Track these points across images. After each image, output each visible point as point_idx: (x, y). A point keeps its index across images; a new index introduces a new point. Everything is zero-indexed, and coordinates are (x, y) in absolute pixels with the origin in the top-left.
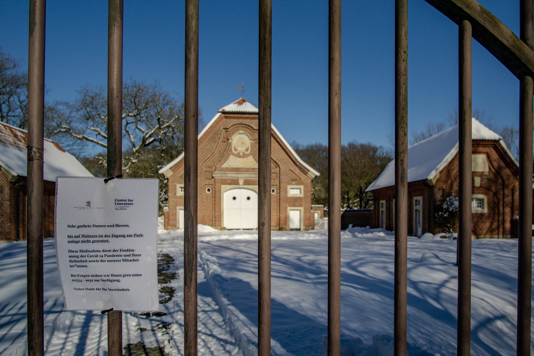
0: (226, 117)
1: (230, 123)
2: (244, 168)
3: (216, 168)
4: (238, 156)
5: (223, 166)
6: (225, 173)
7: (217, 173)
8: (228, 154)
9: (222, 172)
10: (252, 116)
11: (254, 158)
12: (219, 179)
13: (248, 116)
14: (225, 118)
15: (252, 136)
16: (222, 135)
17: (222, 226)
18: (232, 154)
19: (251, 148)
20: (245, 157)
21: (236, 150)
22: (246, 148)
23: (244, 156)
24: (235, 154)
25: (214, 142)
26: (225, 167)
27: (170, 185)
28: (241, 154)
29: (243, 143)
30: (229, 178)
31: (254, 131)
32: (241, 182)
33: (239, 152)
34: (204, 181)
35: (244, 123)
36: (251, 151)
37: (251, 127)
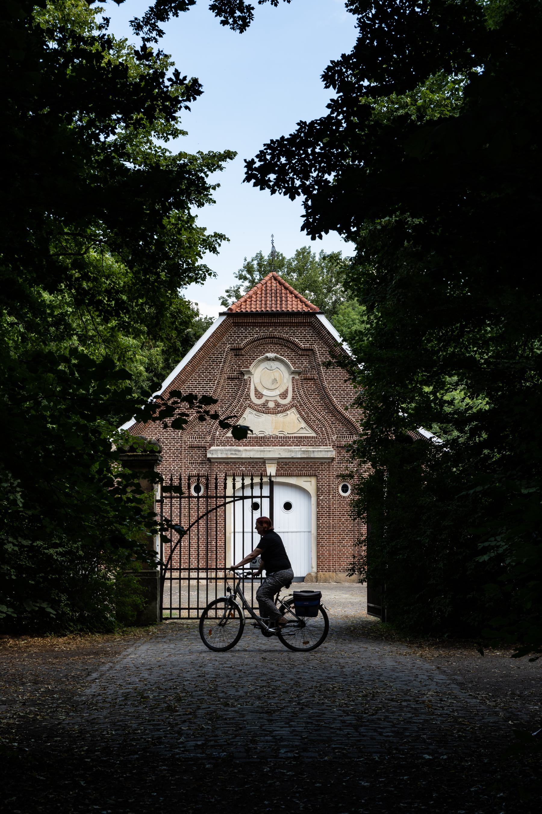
0: (237, 325)
1: (246, 337)
2: (277, 437)
3: (213, 439)
4: (264, 409)
6: (236, 450)
7: (216, 451)
8: (242, 405)
9: (228, 447)
10: (295, 320)
11: (300, 414)
13: (286, 320)
14: (235, 326)
15: (294, 364)
16: (227, 364)
18: (250, 406)
19: (294, 391)
20: (279, 412)
21: (259, 395)
22: (282, 390)
23: (279, 410)
24: (256, 405)
25: (210, 380)
28: (271, 405)
29: (275, 381)
30: (243, 461)
31: (300, 352)
32: (271, 470)
33: (267, 401)
34: (188, 468)
36: (293, 398)
37: (293, 343)
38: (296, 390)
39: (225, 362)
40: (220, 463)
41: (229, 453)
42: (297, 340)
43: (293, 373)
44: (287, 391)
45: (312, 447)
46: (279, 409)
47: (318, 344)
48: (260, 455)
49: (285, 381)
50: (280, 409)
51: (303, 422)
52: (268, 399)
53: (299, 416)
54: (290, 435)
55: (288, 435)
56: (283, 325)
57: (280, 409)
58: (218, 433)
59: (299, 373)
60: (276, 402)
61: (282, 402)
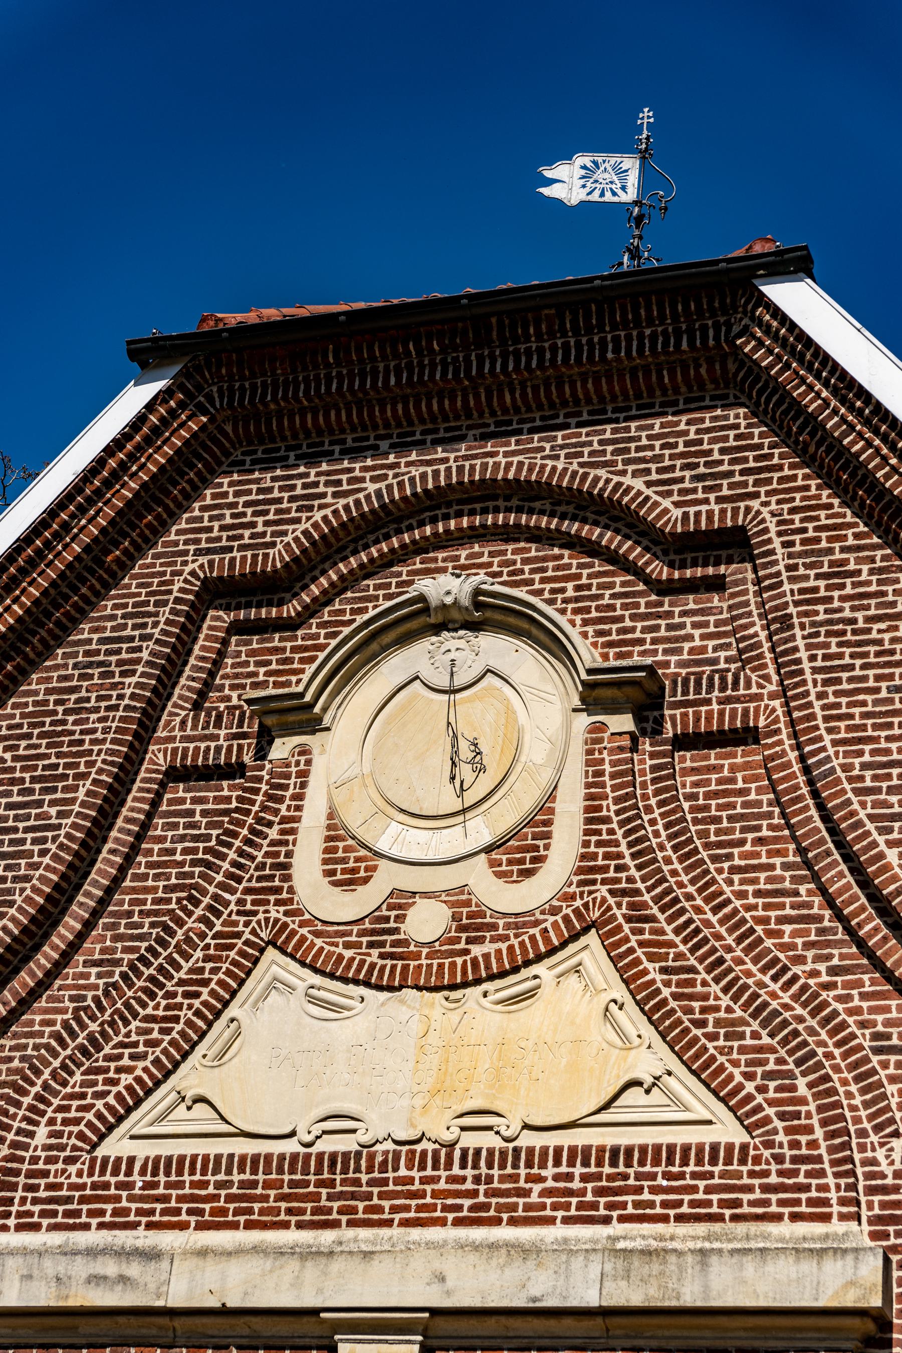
9: (94, 1237)
25: (49, 781)
26: (144, 1150)
38: (609, 808)
41: (81, 1268)
42: (638, 484)
45: (701, 1228)
46: (477, 950)
47: (785, 493)
48: (297, 1283)
50: (489, 947)
51: (649, 1032)
52: (409, 879)
53: (620, 992)
54: (537, 1140)
55: (528, 1140)
57: (489, 947)
58: (42, 1132)
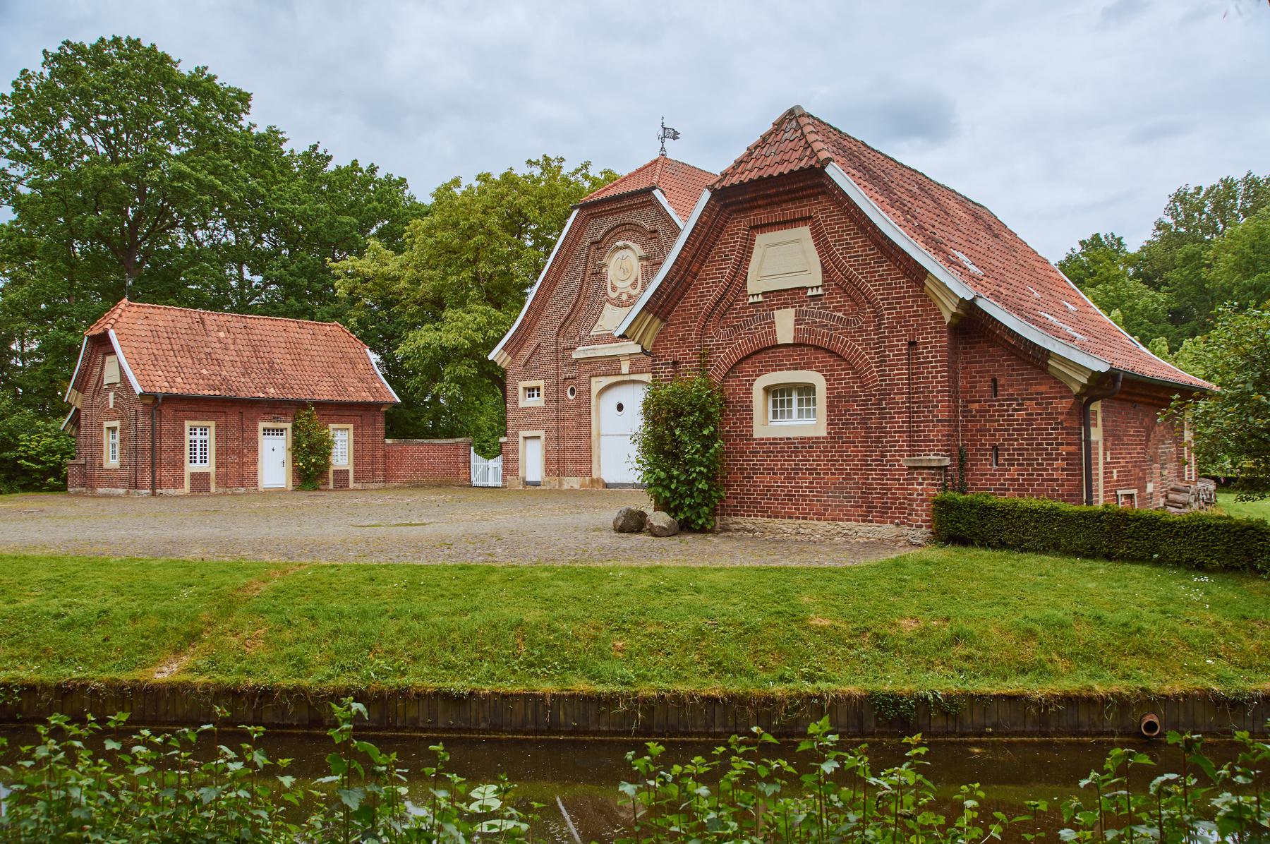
0: (594, 216)
5: (592, 333)
12: (585, 363)
17: (595, 476)
18: (607, 301)
21: (614, 289)
27: (509, 382)
28: (624, 297)
31: (649, 236)
33: (621, 294)
35: (626, 220)
39: (587, 259)
40: (585, 363)
43: (641, 258)
44: (636, 280)
49: (635, 269)
56: (630, 208)
59: (647, 258)
60: (628, 293)
61: (634, 292)
